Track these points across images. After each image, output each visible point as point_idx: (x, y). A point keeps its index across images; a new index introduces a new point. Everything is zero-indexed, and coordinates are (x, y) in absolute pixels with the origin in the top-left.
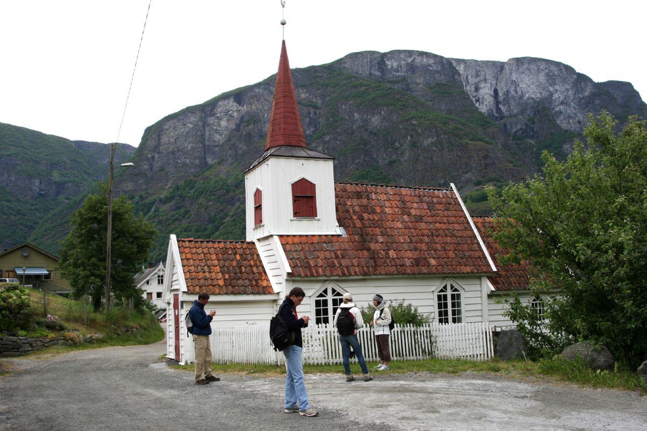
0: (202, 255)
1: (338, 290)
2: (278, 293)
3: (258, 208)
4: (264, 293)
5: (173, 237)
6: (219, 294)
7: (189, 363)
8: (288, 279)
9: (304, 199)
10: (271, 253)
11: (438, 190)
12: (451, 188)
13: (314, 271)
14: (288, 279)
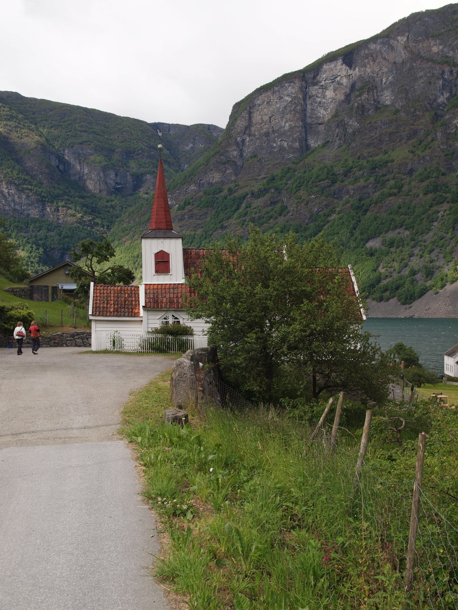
4: (135, 316)
5: (92, 284)
6: (109, 316)
9: (162, 263)
13: (160, 305)
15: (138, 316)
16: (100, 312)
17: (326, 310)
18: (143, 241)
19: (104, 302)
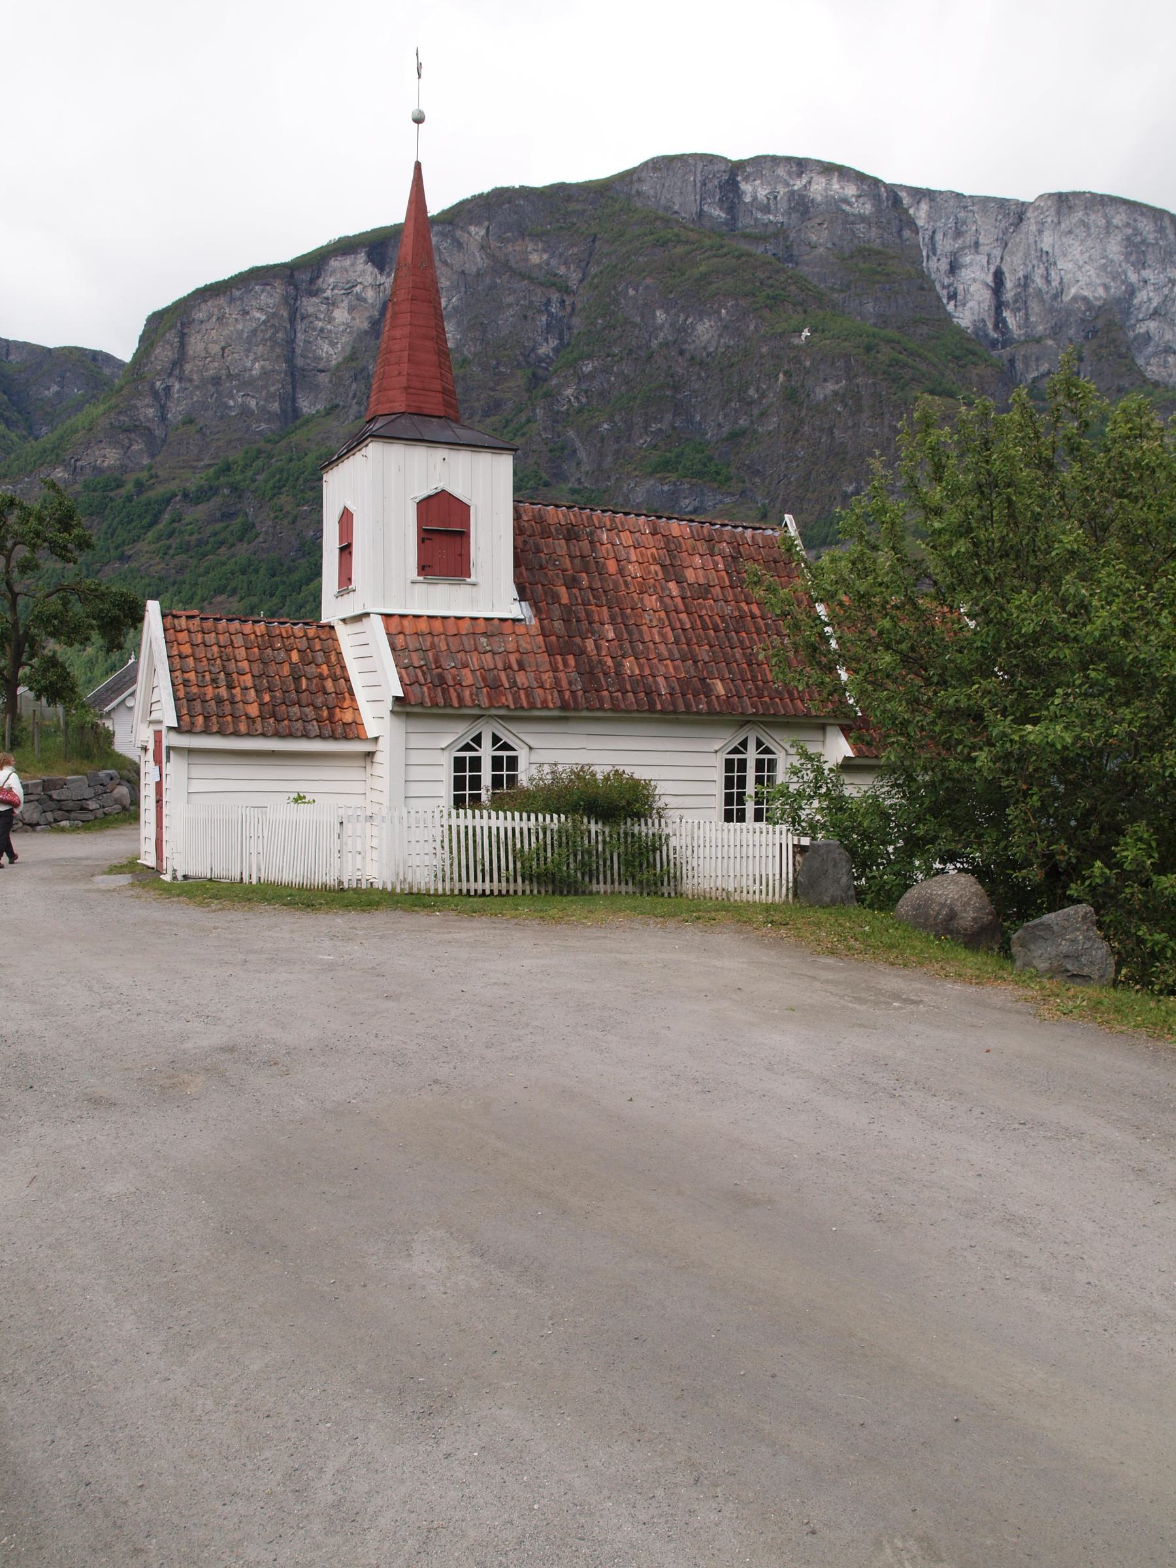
0: (215, 648)
1: (506, 738)
2: (376, 739)
3: (346, 550)
4: (346, 738)
5: (153, 608)
6: (249, 735)
7: (180, 878)
8: (397, 709)
9: (442, 537)
10: (363, 651)
11: (754, 529)
12: (786, 525)
13: (454, 695)
14: (397, 709)
15: (359, 737)
16: (207, 718)
19: (214, 681)
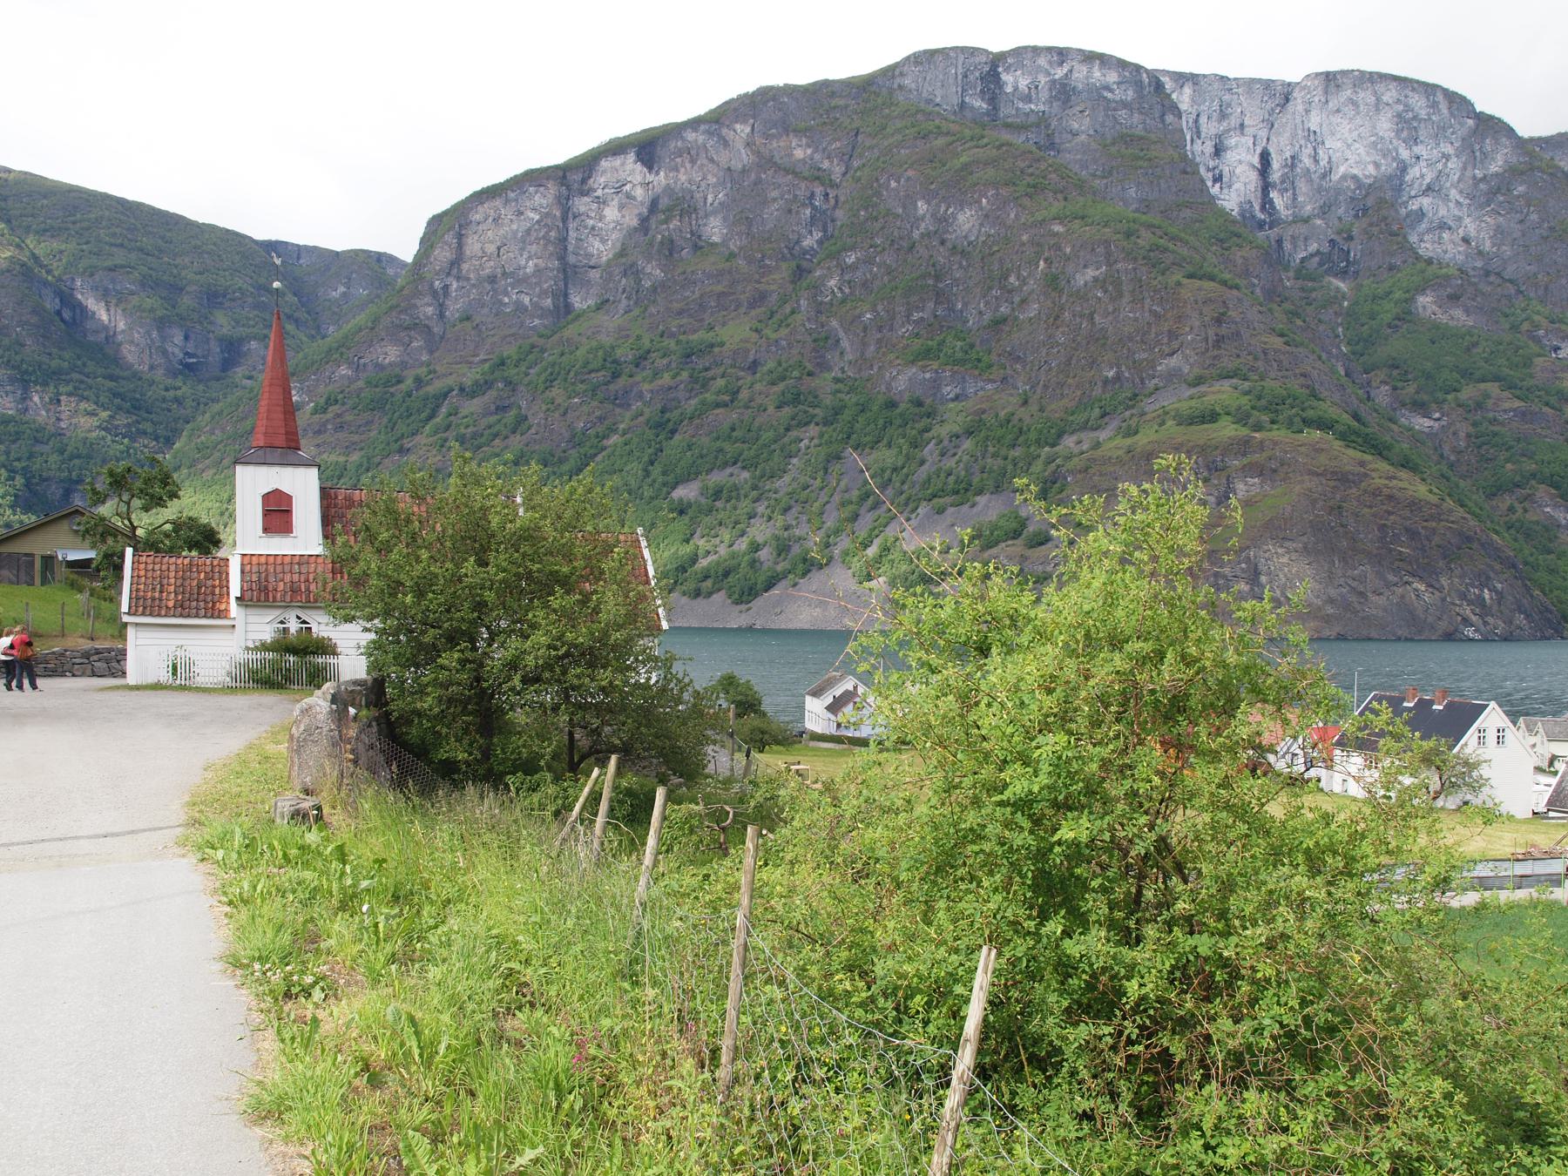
5: (129, 551)
9: (277, 513)
17: (596, 611)
18: (239, 468)
